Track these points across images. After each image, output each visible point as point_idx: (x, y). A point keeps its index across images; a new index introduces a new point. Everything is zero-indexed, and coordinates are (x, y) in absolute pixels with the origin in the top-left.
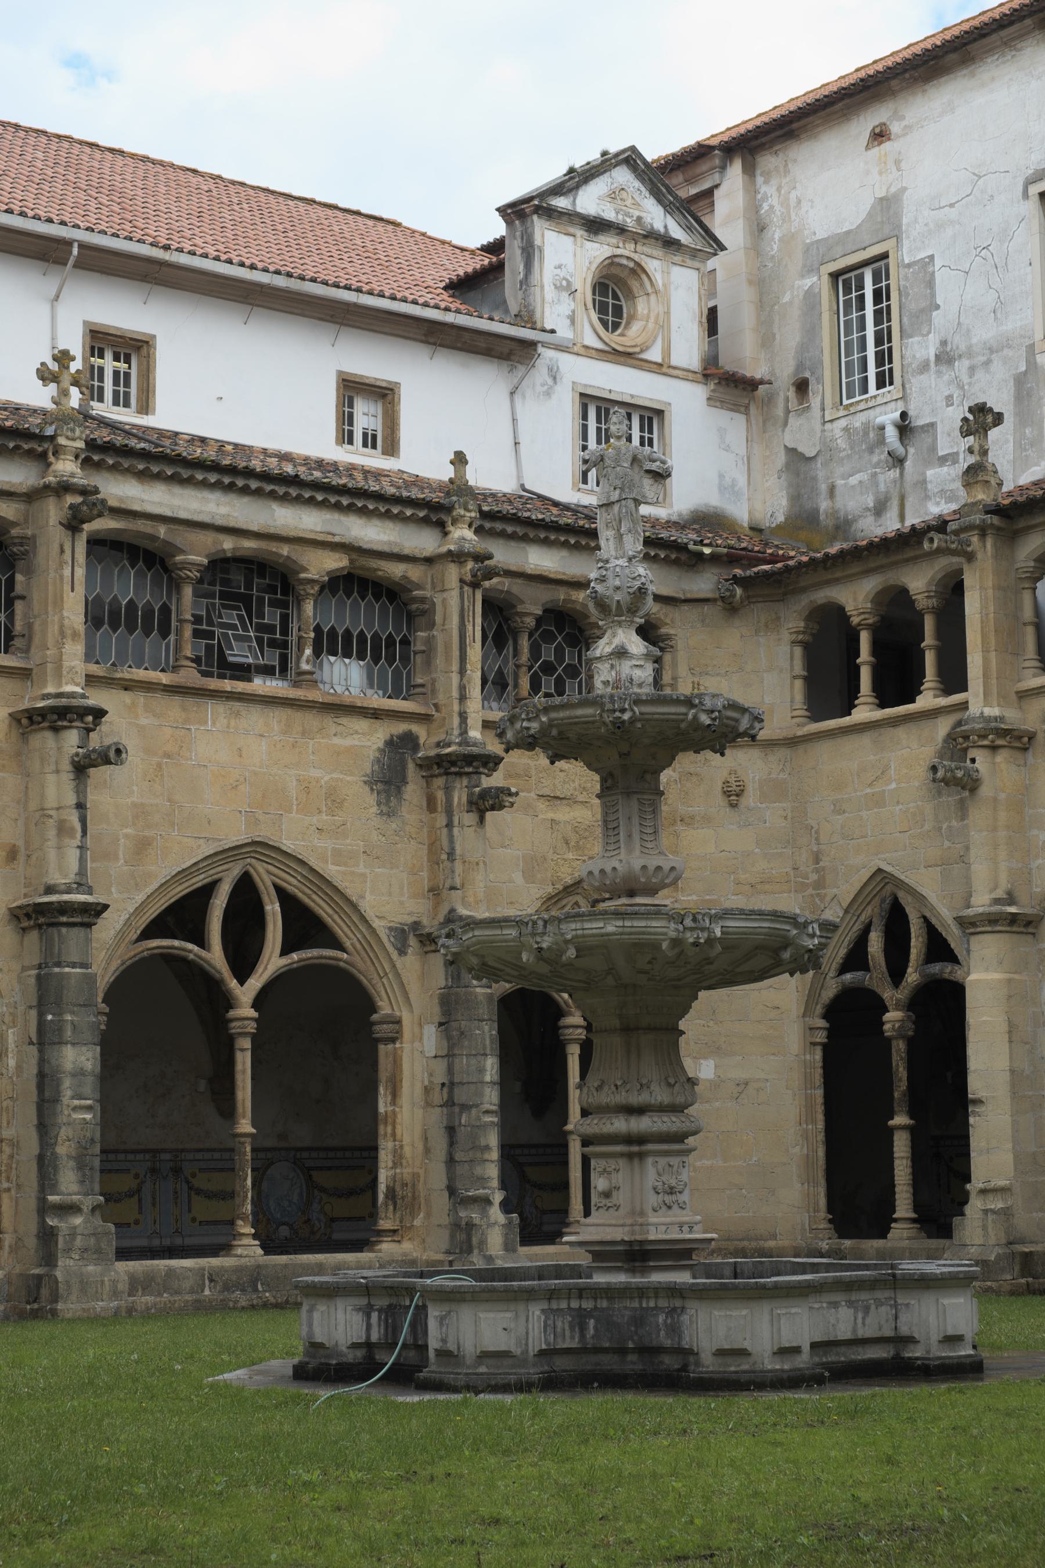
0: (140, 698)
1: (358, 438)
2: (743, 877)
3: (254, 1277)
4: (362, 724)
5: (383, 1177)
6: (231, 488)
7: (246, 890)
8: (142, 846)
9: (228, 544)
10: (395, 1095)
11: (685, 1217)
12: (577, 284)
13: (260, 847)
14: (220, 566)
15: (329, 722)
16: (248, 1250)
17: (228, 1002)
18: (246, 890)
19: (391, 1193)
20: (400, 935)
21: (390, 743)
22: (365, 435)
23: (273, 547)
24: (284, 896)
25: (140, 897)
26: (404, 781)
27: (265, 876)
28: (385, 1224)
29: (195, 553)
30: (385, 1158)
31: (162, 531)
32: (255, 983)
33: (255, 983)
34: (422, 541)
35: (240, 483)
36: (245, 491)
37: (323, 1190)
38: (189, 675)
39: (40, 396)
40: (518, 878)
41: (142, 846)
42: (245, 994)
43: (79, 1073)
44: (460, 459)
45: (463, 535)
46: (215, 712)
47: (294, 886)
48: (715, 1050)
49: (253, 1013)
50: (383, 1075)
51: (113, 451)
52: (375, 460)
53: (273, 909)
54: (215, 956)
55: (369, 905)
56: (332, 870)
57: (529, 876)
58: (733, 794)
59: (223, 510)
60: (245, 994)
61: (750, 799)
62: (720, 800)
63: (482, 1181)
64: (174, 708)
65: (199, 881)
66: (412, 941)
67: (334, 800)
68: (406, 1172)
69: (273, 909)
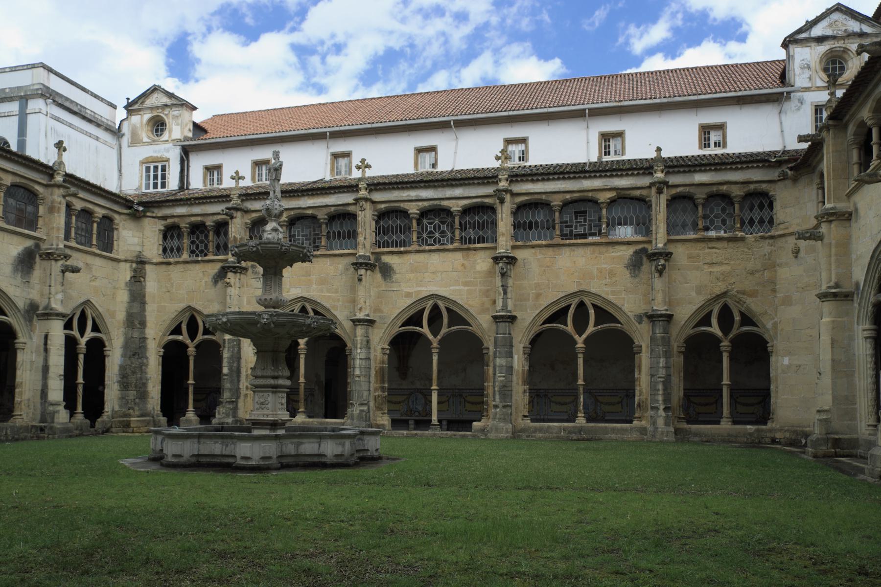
0: (538, 250)
1: (712, 144)
2: (799, 285)
3: (580, 430)
4: (624, 248)
5: (637, 399)
6: (564, 178)
7: (581, 305)
8: (538, 296)
9: (568, 196)
10: (640, 371)
11: (266, 412)
12: (813, 65)
13: (582, 292)
14: (566, 204)
15: (610, 249)
16: (581, 421)
17: (575, 343)
18: (581, 305)
19: (639, 405)
20: (640, 318)
21: (636, 252)
22: (715, 143)
23: (586, 194)
24: (594, 306)
25: (537, 312)
26: (642, 265)
27: (588, 301)
28: (637, 415)
29: (556, 201)
30: (637, 393)
31: (544, 197)
32: (584, 336)
33: (584, 336)
34: (645, 181)
35: (566, 176)
36: (569, 178)
37: (469, 402)
38: (558, 240)
39: (497, 164)
40: (694, 294)
41: (538, 296)
42: (580, 341)
43: (502, 366)
44: (659, 150)
45: (659, 175)
46: (565, 251)
47: (599, 303)
48: (789, 353)
49: (583, 346)
50: (637, 365)
51: (516, 176)
52: (719, 151)
53: (592, 312)
54: (570, 328)
55: (626, 308)
56: (611, 297)
57: (699, 292)
58: (796, 253)
59: (563, 186)
60: (580, 341)
61: (802, 254)
62: (791, 255)
63: (657, 401)
64: (550, 252)
65: (563, 305)
66: (645, 319)
67: (612, 274)
68: (643, 398)
69: (592, 312)
